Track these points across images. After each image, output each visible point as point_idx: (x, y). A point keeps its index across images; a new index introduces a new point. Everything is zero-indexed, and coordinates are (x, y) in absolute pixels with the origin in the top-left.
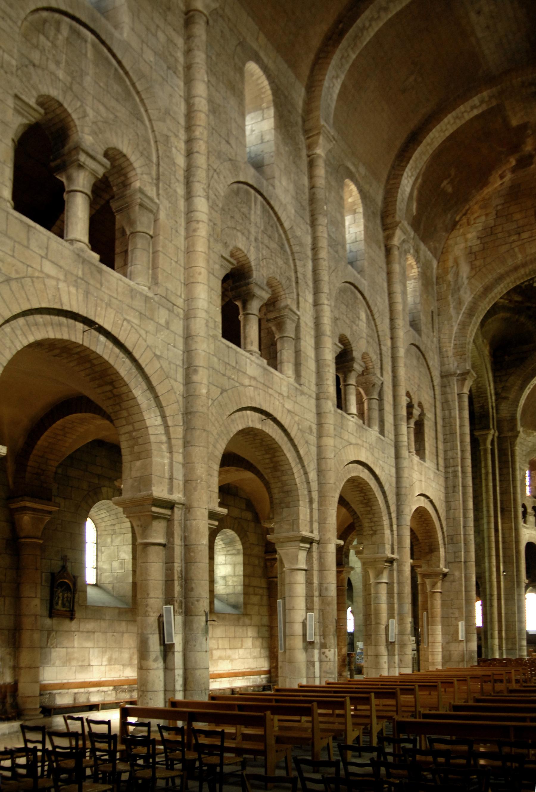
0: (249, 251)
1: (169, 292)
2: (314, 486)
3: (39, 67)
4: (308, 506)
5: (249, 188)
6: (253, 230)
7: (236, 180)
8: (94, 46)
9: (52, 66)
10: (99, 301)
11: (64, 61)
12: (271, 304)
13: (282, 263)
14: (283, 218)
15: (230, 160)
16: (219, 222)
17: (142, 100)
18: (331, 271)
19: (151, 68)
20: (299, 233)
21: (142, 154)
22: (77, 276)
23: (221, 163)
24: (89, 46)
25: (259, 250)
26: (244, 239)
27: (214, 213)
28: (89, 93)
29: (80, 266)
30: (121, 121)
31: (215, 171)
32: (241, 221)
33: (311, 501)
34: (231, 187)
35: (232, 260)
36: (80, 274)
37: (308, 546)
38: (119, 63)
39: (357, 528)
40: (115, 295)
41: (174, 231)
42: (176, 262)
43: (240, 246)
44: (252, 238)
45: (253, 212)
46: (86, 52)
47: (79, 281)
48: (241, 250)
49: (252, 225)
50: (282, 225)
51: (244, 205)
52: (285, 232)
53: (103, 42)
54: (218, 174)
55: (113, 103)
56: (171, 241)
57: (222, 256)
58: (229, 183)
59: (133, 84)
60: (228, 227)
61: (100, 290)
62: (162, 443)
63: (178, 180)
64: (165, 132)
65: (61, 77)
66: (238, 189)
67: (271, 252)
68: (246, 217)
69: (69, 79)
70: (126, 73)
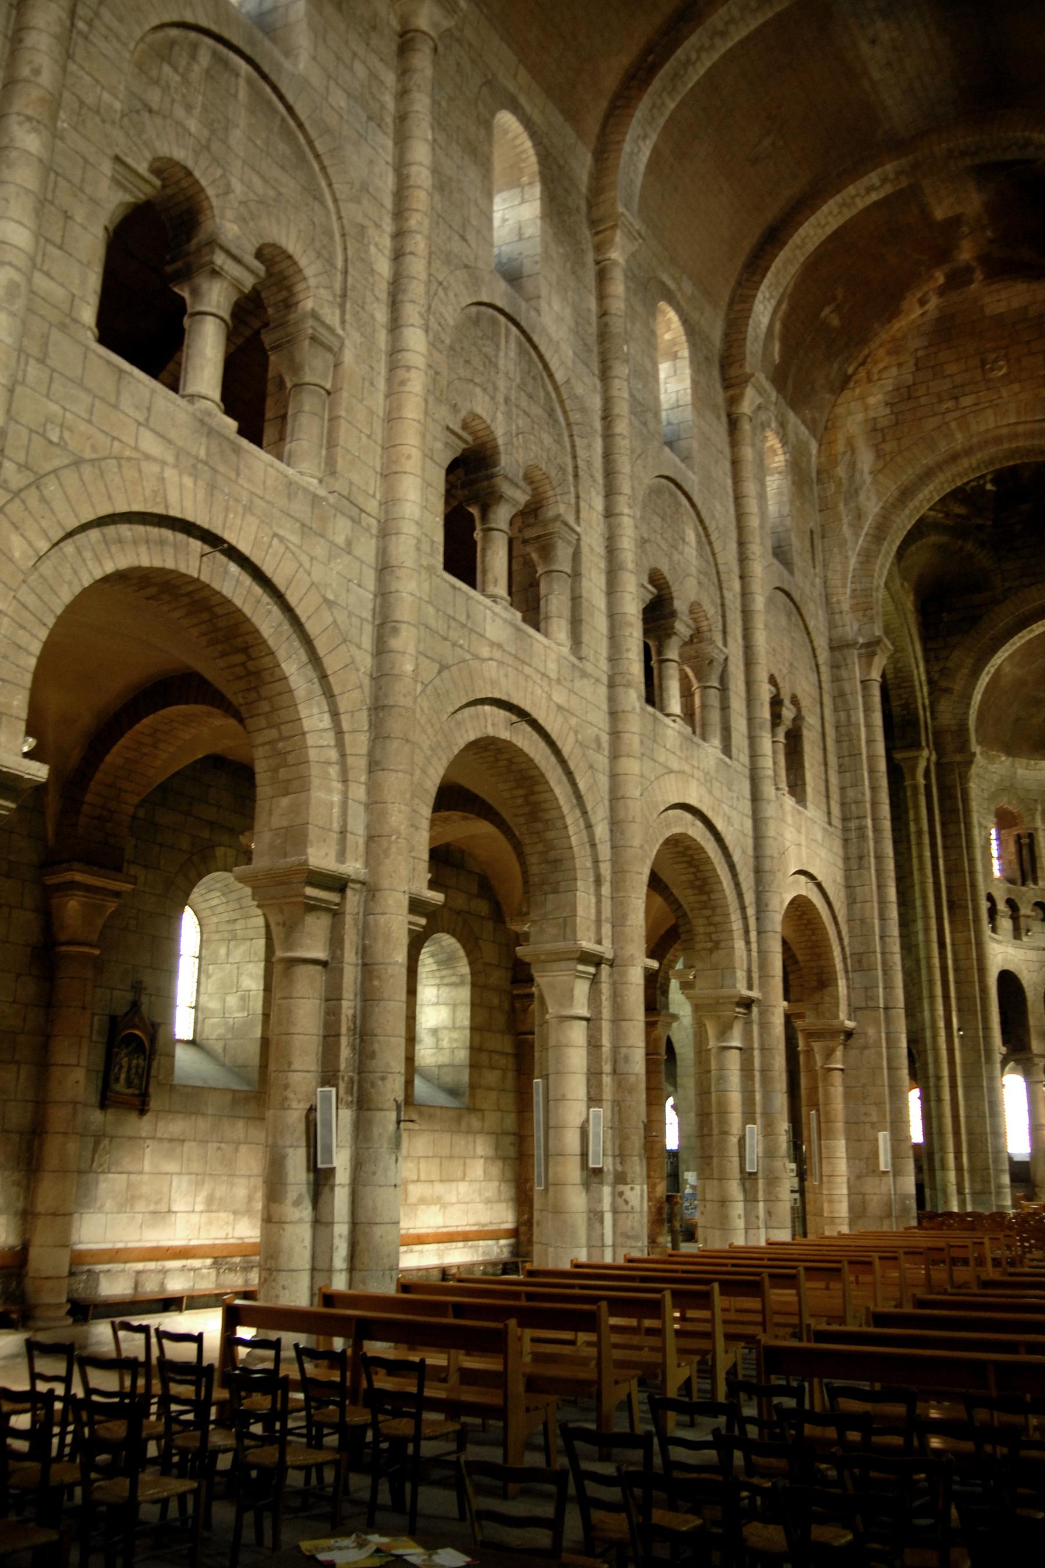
0: (494, 419)
1: (354, 489)
2: (605, 851)
3: (158, 113)
4: (592, 890)
5: (496, 313)
6: (502, 384)
7: (475, 300)
8: (250, 82)
9: (179, 112)
10: (231, 503)
11: (199, 104)
12: (531, 513)
13: (551, 440)
14: (554, 364)
15: (466, 266)
16: (444, 370)
17: (323, 168)
18: (635, 456)
19: (341, 117)
20: (580, 390)
21: (319, 255)
22: (197, 458)
23: (452, 272)
24: (242, 83)
25: (511, 418)
26: (487, 398)
27: (436, 354)
28: (237, 156)
29: (204, 440)
30: (288, 201)
31: (440, 284)
32: (481, 368)
33: (598, 882)
34: (467, 311)
35: (465, 435)
36: (202, 454)
38: (290, 109)
39: (683, 936)
40: (260, 492)
41: (367, 384)
42: (369, 437)
43: (479, 410)
44: (500, 398)
45: (502, 354)
46: (237, 91)
47: (200, 466)
48: (480, 418)
49: (501, 375)
50: (551, 376)
51: (488, 342)
52: (556, 388)
53: (265, 77)
54: (445, 289)
55: (276, 172)
56: (361, 401)
57: (448, 428)
58: (464, 304)
59: (310, 143)
60: (460, 379)
61: (236, 482)
63: (378, 299)
64: (360, 219)
65: (193, 129)
66: (478, 314)
67: (533, 422)
68: (490, 362)
69: (206, 133)
70: (300, 125)
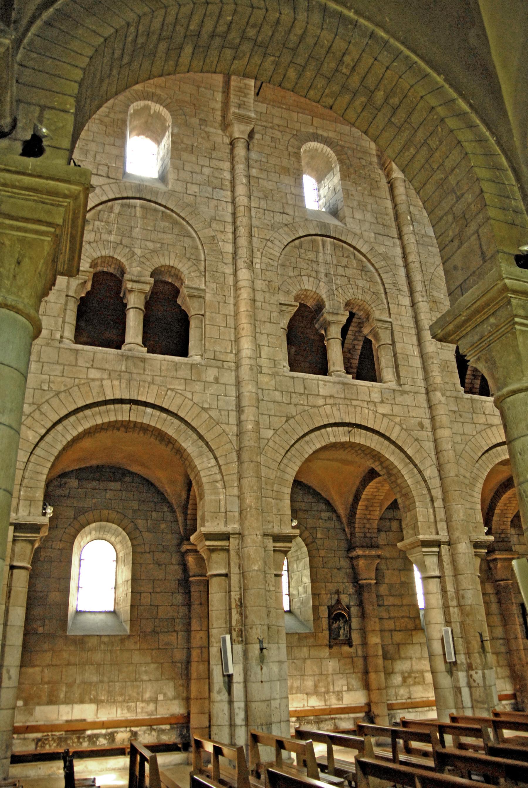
17: (187, 222)
37: (436, 549)
59: (178, 215)
62: (217, 482)
70: (172, 211)
